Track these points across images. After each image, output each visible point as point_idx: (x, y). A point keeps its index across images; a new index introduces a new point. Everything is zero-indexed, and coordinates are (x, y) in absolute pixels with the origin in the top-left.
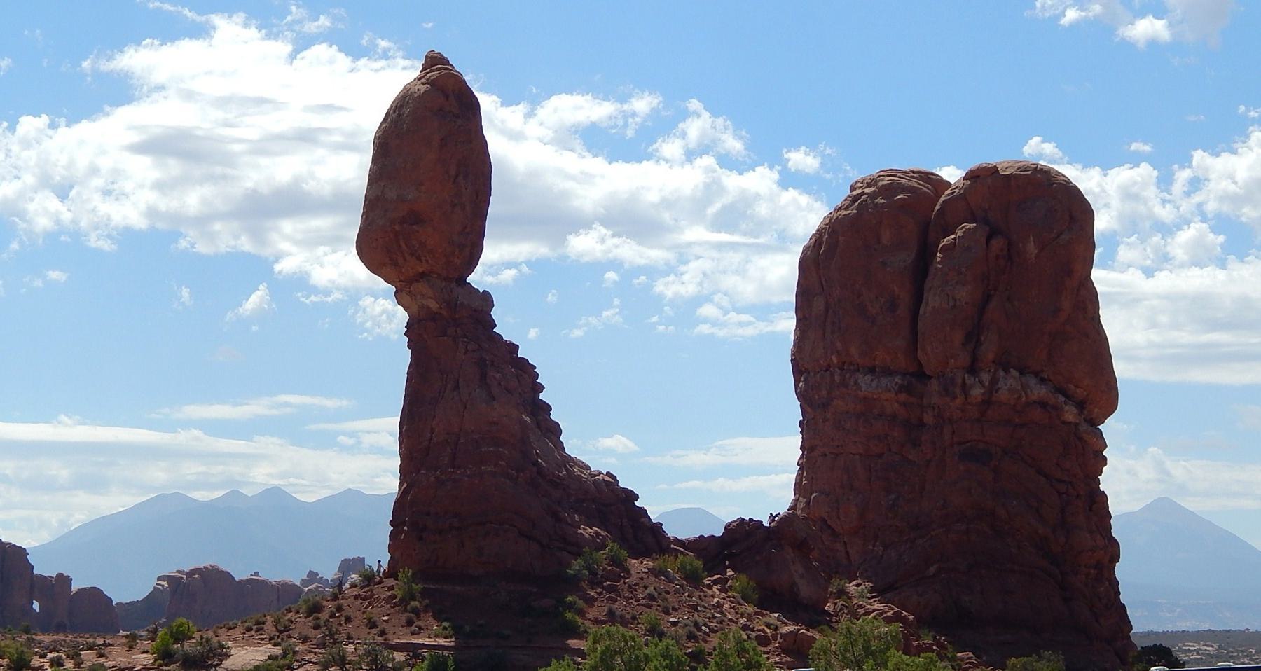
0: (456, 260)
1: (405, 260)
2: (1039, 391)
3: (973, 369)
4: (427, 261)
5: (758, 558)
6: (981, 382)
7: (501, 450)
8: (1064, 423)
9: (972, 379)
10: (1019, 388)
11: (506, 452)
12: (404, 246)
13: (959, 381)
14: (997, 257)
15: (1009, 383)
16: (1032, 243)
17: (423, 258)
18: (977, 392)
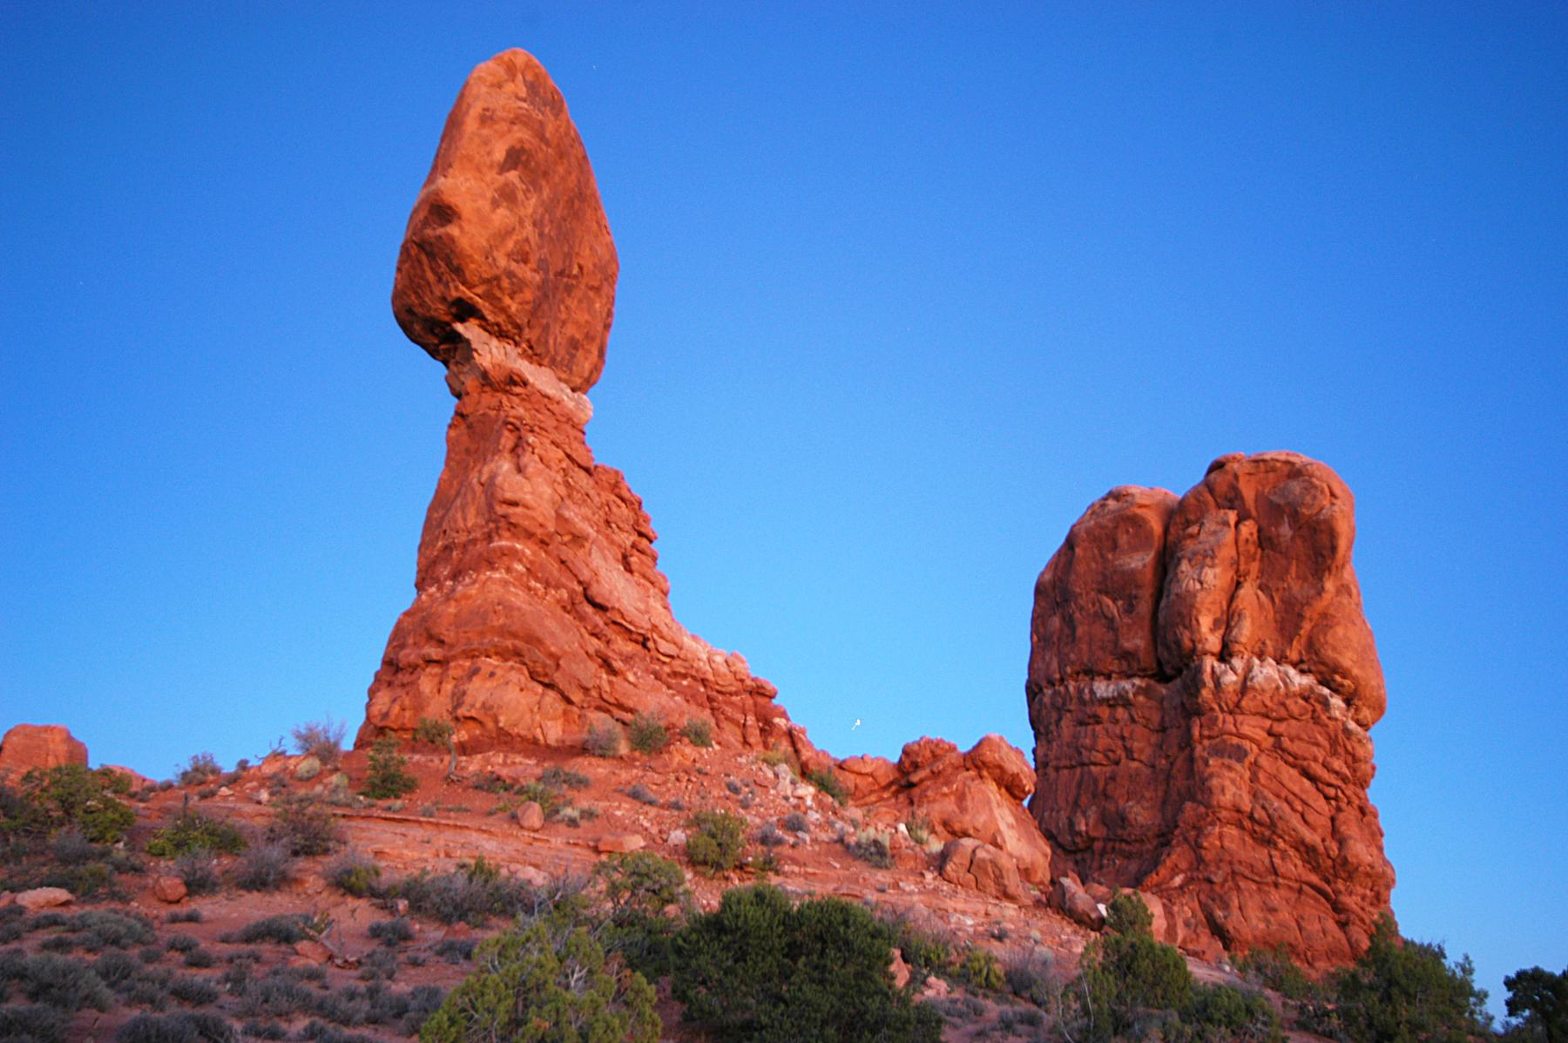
0: (507, 301)
1: (432, 292)
2: (1299, 681)
3: (1224, 655)
4: (457, 288)
5: (945, 790)
6: (1232, 669)
7: (518, 546)
8: (1329, 718)
9: (1223, 666)
10: (1277, 677)
11: (528, 552)
12: (427, 268)
13: (1208, 669)
14: (1247, 541)
15: (1266, 672)
16: (1287, 525)
17: (451, 285)
18: (1230, 679)
